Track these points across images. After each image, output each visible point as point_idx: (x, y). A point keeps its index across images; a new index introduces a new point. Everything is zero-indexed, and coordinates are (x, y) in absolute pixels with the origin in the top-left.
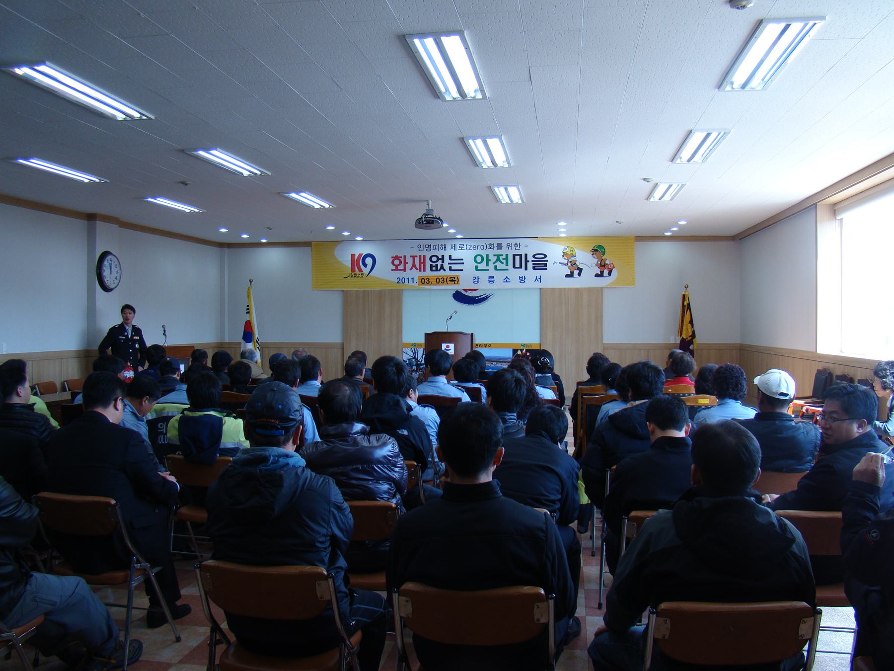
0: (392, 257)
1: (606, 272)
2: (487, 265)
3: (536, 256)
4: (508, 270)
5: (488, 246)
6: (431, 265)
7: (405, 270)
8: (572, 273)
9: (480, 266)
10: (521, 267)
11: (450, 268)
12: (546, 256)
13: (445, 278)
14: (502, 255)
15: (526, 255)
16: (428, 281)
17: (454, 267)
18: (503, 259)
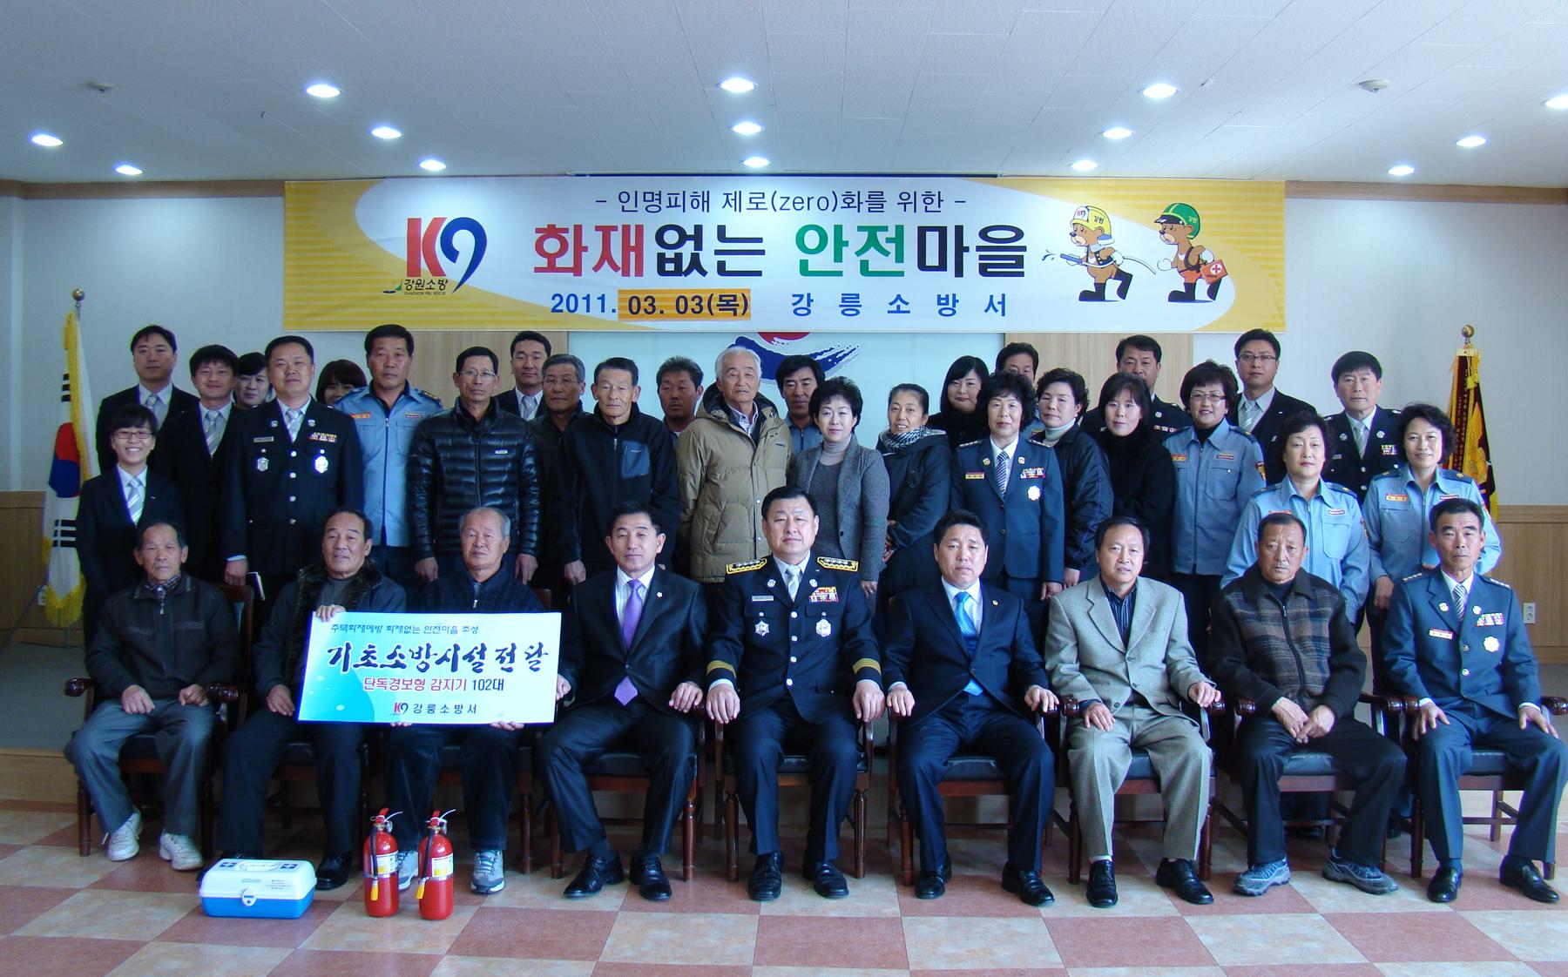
0: (538, 231)
1: (1202, 288)
2: (838, 258)
3: (991, 234)
4: (901, 274)
5: (840, 199)
7: (577, 270)
9: (816, 262)
10: (942, 266)
11: (721, 266)
12: (1019, 234)
13: (705, 297)
14: (885, 229)
15: (959, 230)
16: (652, 305)
17: (733, 263)
18: (888, 240)
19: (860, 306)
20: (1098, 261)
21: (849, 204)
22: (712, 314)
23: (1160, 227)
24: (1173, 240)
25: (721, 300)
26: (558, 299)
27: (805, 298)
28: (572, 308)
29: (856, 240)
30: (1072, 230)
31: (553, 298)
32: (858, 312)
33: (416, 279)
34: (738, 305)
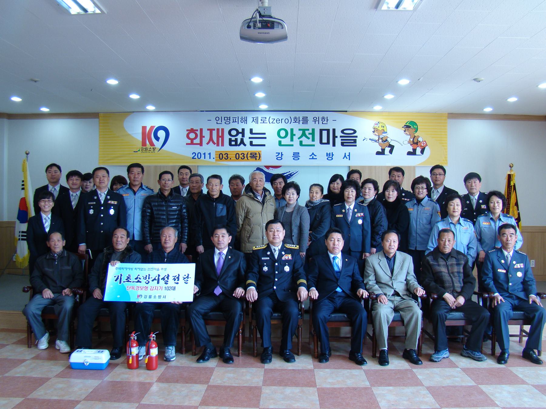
0: (187, 130)
1: (418, 150)
2: (292, 140)
3: (345, 132)
4: (314, 145)
5: (293, 119)
6: (230, 140)
7: (201, 144)
8: (383, 150)
9: (284, 142)
10: (328, 143)
11: (251, 143)
12: (355, 132)
13: (246, 153)
14: (308, 130)
15: (334, 130)
17: (255, 142)
18: (309, 134)
19: (300, 157)
20: (382, 141)
21: (295, 121)
22: (248, 159)
23: (404, 129)
24: (408, 134)
25: (251, 155)
26: (194, 154)
27: (280, 154)
28: (199, 157)
29: (298, 134)
30: (373, 130)
31: (193, 154)
32: (299, 159)
33: (145, 147)
34: (257, 156)
